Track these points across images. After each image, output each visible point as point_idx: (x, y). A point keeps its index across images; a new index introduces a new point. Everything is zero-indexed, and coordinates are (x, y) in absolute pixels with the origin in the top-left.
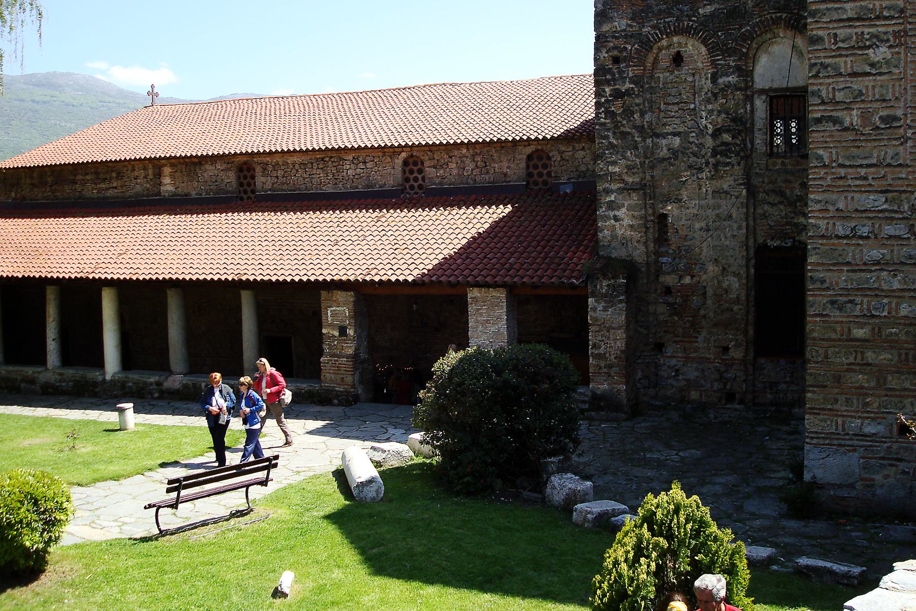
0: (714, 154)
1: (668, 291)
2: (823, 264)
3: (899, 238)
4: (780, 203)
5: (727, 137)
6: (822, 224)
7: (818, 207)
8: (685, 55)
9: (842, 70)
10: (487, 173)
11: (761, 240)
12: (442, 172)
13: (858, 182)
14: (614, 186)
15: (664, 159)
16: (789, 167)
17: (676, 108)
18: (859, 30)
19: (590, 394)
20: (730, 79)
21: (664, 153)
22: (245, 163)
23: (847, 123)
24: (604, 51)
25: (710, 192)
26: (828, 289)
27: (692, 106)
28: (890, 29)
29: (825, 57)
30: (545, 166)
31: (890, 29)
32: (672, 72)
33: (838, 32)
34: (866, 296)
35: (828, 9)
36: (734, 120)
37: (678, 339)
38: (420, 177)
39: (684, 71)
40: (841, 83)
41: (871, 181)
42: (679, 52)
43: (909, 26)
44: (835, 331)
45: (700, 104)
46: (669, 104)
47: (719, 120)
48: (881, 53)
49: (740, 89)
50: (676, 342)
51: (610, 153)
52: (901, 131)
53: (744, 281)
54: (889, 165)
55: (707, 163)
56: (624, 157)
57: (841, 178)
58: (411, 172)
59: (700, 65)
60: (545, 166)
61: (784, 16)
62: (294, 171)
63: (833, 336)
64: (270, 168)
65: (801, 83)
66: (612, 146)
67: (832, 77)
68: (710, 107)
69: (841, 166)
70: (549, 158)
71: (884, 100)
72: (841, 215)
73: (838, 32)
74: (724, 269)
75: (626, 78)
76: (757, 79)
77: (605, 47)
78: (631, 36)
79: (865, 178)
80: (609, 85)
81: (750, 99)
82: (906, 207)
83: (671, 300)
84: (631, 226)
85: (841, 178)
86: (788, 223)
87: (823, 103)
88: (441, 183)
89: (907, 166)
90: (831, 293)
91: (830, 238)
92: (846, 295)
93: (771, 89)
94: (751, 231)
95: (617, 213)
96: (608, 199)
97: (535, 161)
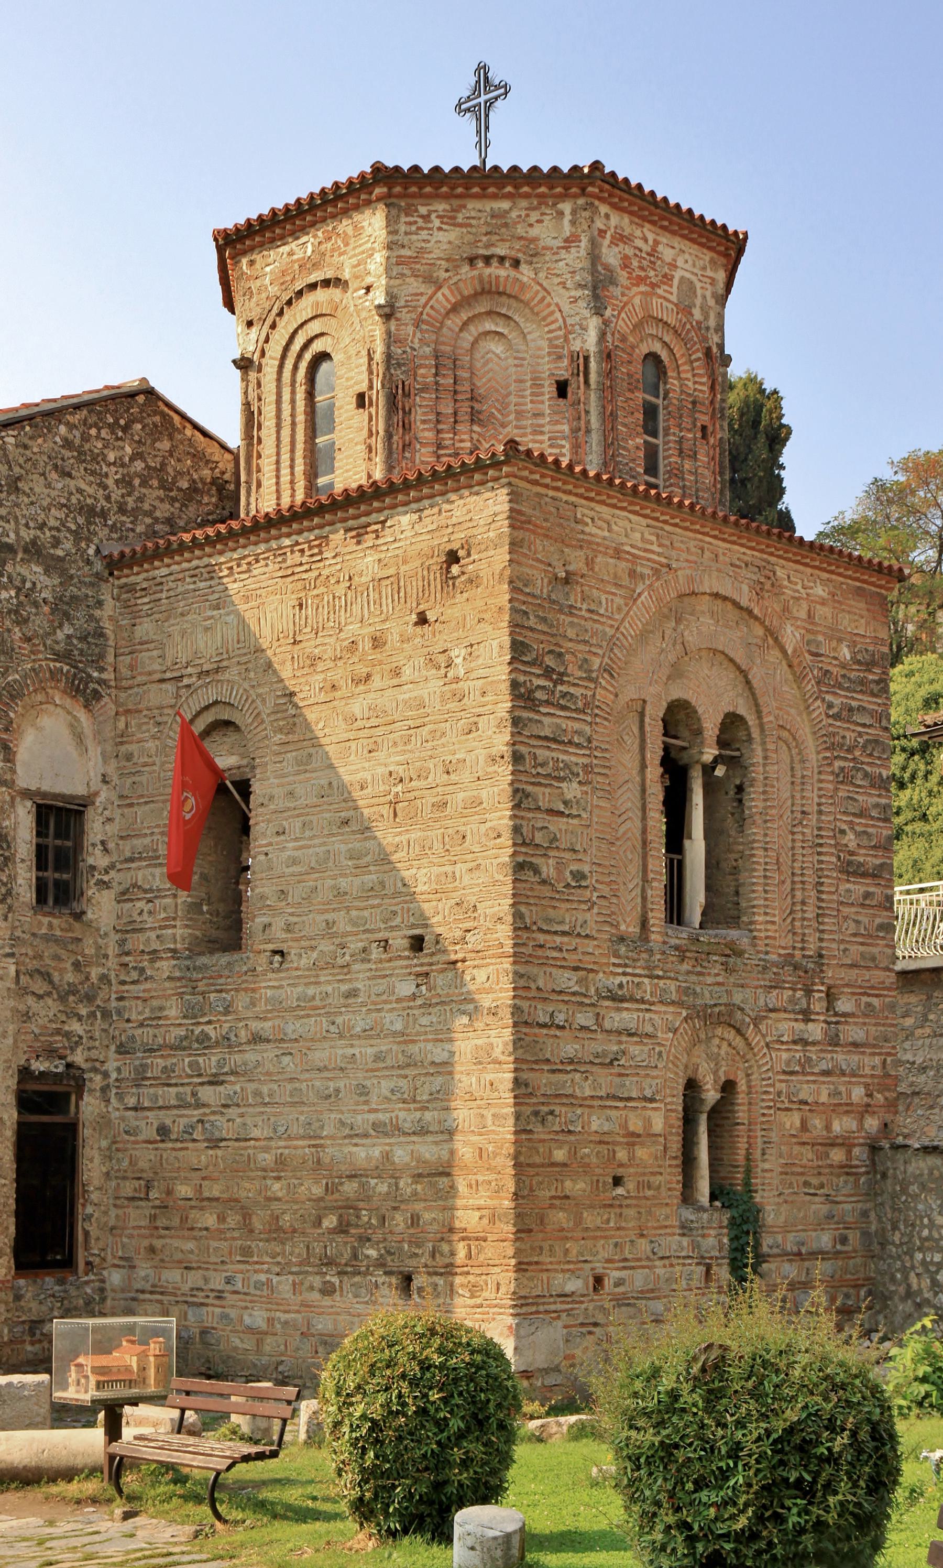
9: (541, 804)
23: (544, 876)
28: (581, 760)
29: (526, 782)
31: (581, 760)
33: (539, 752)
35: (530, 720)
41: (565, 955)
43: (595, 762)
48: (572, 790)
57: (541, 946)
69: (540, 930)
71: (574, 851)
73: (539, 752)
79: (561, 950)
85: (541, 946)
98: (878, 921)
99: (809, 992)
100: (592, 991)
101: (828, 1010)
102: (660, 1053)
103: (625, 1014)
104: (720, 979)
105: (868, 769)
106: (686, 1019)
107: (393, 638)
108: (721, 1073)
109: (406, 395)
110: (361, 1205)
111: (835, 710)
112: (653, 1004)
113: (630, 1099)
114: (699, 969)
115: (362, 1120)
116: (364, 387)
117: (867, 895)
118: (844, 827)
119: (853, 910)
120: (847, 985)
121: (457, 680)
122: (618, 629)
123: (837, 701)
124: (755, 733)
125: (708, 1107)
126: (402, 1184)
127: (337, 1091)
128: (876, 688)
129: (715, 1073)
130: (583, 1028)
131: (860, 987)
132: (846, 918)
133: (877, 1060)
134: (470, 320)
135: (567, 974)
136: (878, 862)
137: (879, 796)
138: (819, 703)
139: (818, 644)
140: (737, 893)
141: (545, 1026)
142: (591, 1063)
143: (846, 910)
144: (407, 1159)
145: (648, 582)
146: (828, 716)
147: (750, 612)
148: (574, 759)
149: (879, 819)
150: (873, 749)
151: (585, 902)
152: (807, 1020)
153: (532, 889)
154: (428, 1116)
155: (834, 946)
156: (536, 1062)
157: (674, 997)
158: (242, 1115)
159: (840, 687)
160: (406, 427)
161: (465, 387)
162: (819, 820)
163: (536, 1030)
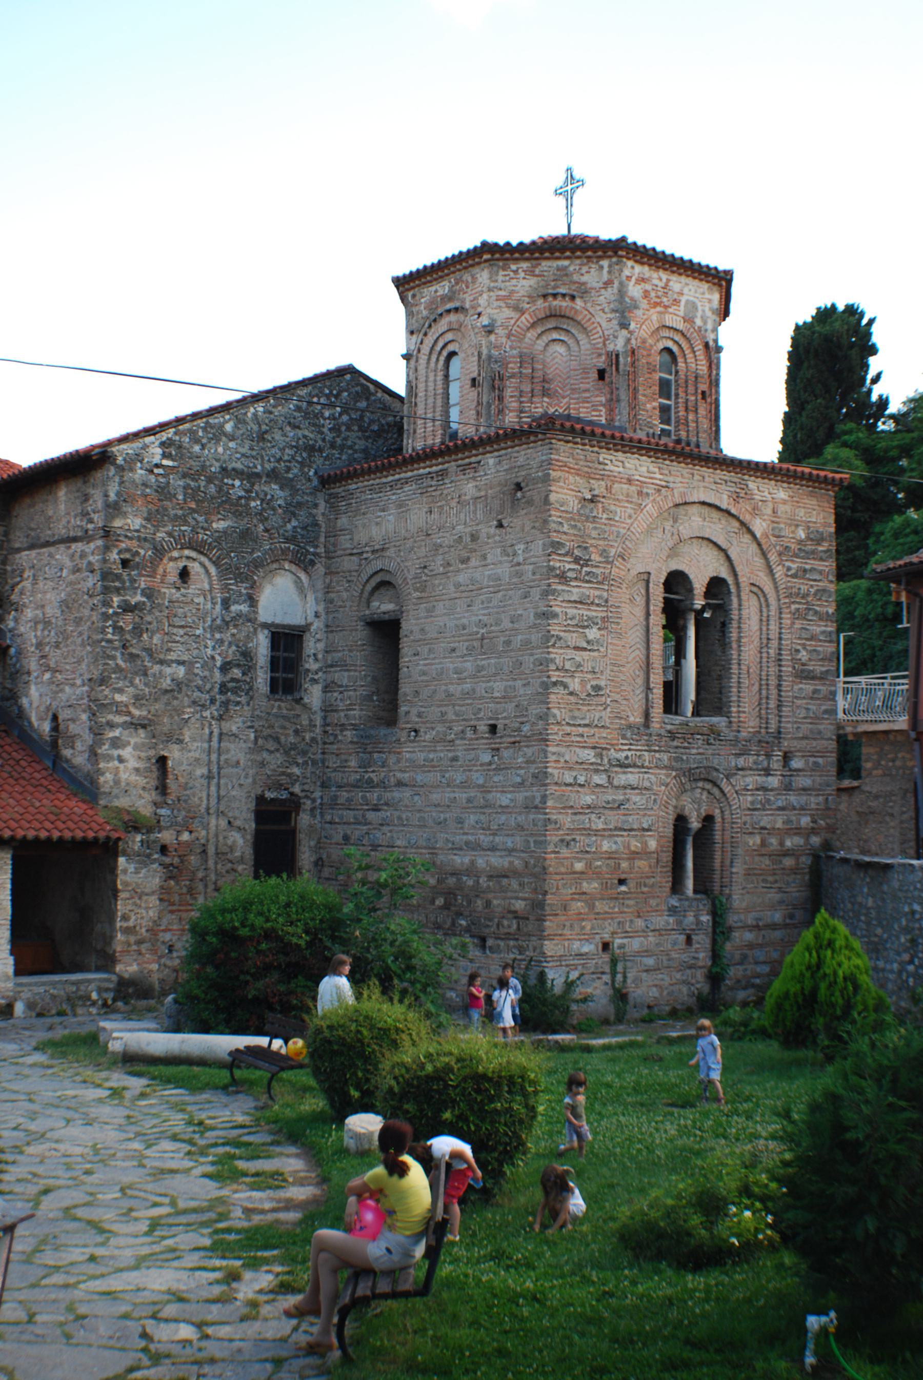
0: (221, 692)
1: (164, 849)
4: (277, 750)
6: (555, 772)
7: (554, 758)
8: (192, 572)
13: (578, 739)
14: (119, 719)
15: (166, 691)
16: (285, 711)
17: (181, 632)
18: (581, 612)
19: (114, 978)
21: (166, 683)
23: (571, 689)
24: (115, 551)
32: (178, 589)
33: (568, 611)
37: (174, 908)
39: (192, 589)
40: (571, 653)
44: (563, 865)
45: (204, 629)
46: (174, 626)
47: (230, 652)
48: (593, 633)
50: (172, 912)
51: (118, 678)
52: (603, 699)
55: (213, 701)
56: (132, 684)
61: (292, 547)
63: (563, 870)
65: (303, 623)
66: (118, 669)
68: (218, 636)
69: (568, 724)
73: (568, 611)
74: (229, 822)
75: (137, 588)
76: (261, 610)
77: (117, 546)
79: (583, 736)
80: (119, 594)
83: (167, 860)
84: (137, 770)
86: (283, 773)
87: (558, 669)
90: (561, 832)
93: (273, 625)
96: (111, 735)
98: (823, 708)
99: (768, 756)
100: (606, 761)
101: (784, 767)
103: (629, 775)
104: (701, 751)
105: (818, 608)
107: (483, 535)
108: (702, 811)
109: (501, 379)
110: (457, 892)
111: (793, 572)
114: (686, 745)
115: (459, 839)
116: (475, 375)
117: (815, 691)
118: (799, 647)
121: (519, 564)
123: (794, 566)
124: (733, 589)
125: (693, 833)
126: (481, 881)
127: (445, 820)
129: (698, 810)
130: (598, 785)
132: (798, 707)
133: (821, 798)
134: (543, 332)
135: (587, 751)
136: (824, 669)
139: (780, 530)
140: (721, 693)
143: (799, 702)
144: (484, 865)
146: (787, 576)
147: (728, 512)
148: (594, 614)
154: (497, 839)
155: (789, 725)
156: (564, 808)
158: (391, 831)
159: (797, 556)
160: (501, 399)
161: (539, 374)
162: (780, 644)
163: (564, 788)
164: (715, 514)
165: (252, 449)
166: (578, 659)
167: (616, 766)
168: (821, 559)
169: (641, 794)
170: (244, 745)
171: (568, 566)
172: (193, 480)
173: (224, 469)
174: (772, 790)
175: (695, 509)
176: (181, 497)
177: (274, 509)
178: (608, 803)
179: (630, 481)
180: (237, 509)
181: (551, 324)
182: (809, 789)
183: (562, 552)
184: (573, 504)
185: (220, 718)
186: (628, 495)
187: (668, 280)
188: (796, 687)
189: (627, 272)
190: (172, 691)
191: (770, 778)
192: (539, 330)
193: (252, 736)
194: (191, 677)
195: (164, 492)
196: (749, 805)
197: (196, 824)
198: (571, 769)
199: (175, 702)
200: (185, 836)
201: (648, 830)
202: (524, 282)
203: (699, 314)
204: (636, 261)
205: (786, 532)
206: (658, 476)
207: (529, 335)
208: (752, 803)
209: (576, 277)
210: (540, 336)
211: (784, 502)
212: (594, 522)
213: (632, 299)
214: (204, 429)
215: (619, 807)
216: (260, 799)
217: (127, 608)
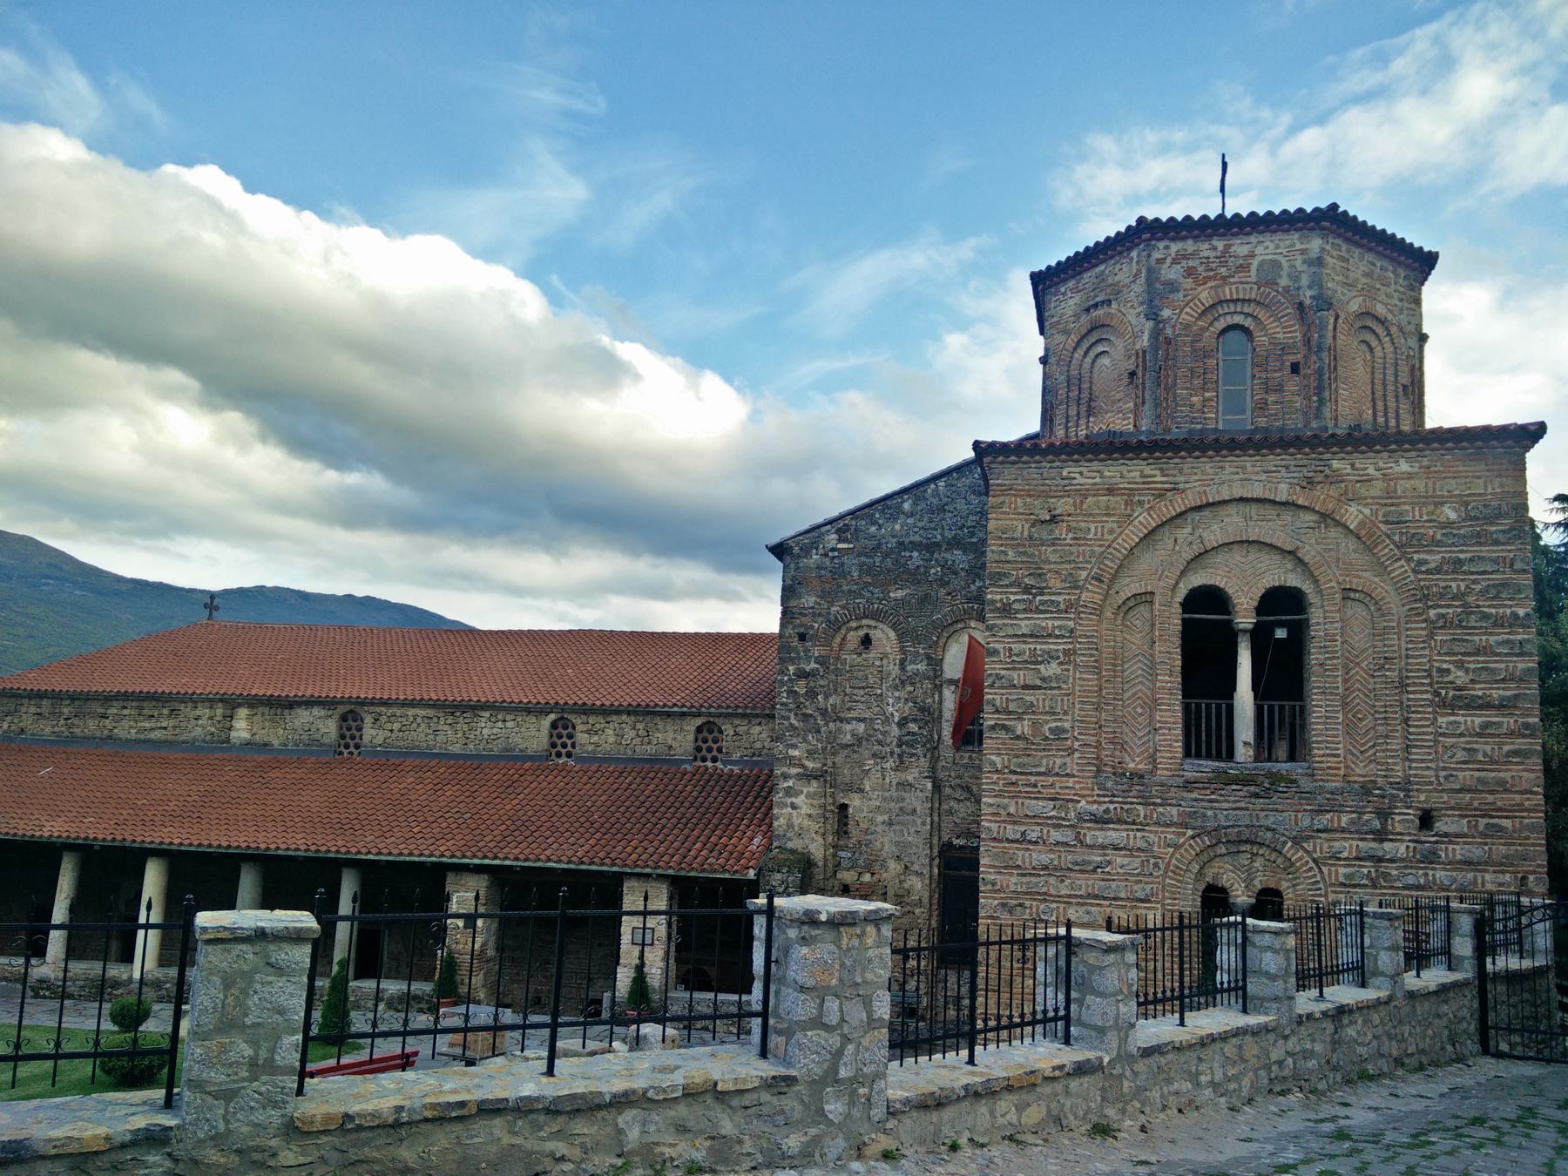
0: (899, 746)
2: (994, 867)
3: (1066, 844)
5: (913, 727)
6: (994, 826)
7: (990, 810)
10: (649, 743)
11: (945, 838)
12: (596, 738)
14: (794, 771)
15: (848, 746)
17: (862, 692)
18: (1032, 647)
20: (919, 666)
22: (351, 711)
23: (1019, 732)
25: (894, 784)
26: (999, 891)
27: (879, 692)
28: (1061, 647)
30: (715, 741)
31: (1061, 647)
34: (1035, 900)
35: (1006, 625)
36: (922, 709)
38: (569, 742)
39: (873, 654)
42: (867, 635)
46: (854, 688)
48: (1052, 669)
49: (929, 678)
53: (927, 882)
54: (1057, 774)
55: (892, 753)
56: (805, 741)
58: (560, 736)
59: (888, 649)
60: (715, 741)
62: (415, 725)
64: (384, 719)
67: (1006, 688)
69: (1015, 773)
70: (721, 732)
72: (1012, 819)
74: (906, 867)
76: (946, 667)
78: (820, 615)
79: (1035, 786)
80: (794, 664)
81: (938, 688)
82: (1073, 815)
84: (810, 816)
87: (997, 711)
88: (594, 752)
89: (1074, 776)
91: (1001, 841)
92: (1016, 899)
94: (936, 828)
95: (794, 800)
96: (785, 785)
97: (705, 734)
98: (1506, 748)
99: (1384, 815)
102: (1156, 865)
105: (1493, 611)
106: (1193, 837)
112: (1148, 825)
113: (1114, 899)
118: (1445, 666)
119: (1462, 739)
120: (1452, 808)
122: (1109, 546)
124: (1313, 598)
128: (1502, 538)
129: (1249, 883)
131: (1476, 809)
136: (1509, 693)
137: (1509, 633)
138: (1403, 562)
141: (1017, 841)
142: (1069, 869)
145: (1147, 506)
149: (1506, 655)
150: (1499, 592)
151: (1064, 750)
152: (1382, 841)
153: (1004, 744)
157: (1175, 819)
159: (1438, 543)
164: (1271, 512)
165: (931, 521)
166: (1027, 698)
167: (1090, 821)
168: (1497, 543)
169: (1132, 856)
170: (920, 794)
171: (1013, 598)
172: (867, 557)
173: (902, 543)
174: (1392, 860)
175: (1232, 509)
176: (856, 574)
177: (955, 573)
178: (1077, 864)
179: (1111, 491)
180: (914, 577)
181: (1092, 339)
182: (1480, 864)
183: (1006, 582)
184: (1021, 528)
185: (896, 770)
186: (1108, 508)
187: (1227, 247)
188: (1442, 720)
189: (1156, 255)
190: (853, 745)
191: (1387, 846)
192: (1084, 347)
193: (929, 786)
194: (871, 732)
195: (840, 573)
196: (1342, 879)
197: (877, 867)
198: (1015, 823)
199: (855, 756)
200: (867, 878)
201: (1142, 901)
202: (1071, 302)
203: (1284, 273)
204: (1173, 239)
205: (1411, 512)
206: (1159, 479)
207: (1076, 355)
208: (1349, 876)
209: (1110, 281)
210: (1086, 353)
211: (1410, 476)
212: (1053, 544)
213: (1165, 283)
214: (882, 511)
215: (1094, 871)
216: (946, 848)
217: (802, 674)
